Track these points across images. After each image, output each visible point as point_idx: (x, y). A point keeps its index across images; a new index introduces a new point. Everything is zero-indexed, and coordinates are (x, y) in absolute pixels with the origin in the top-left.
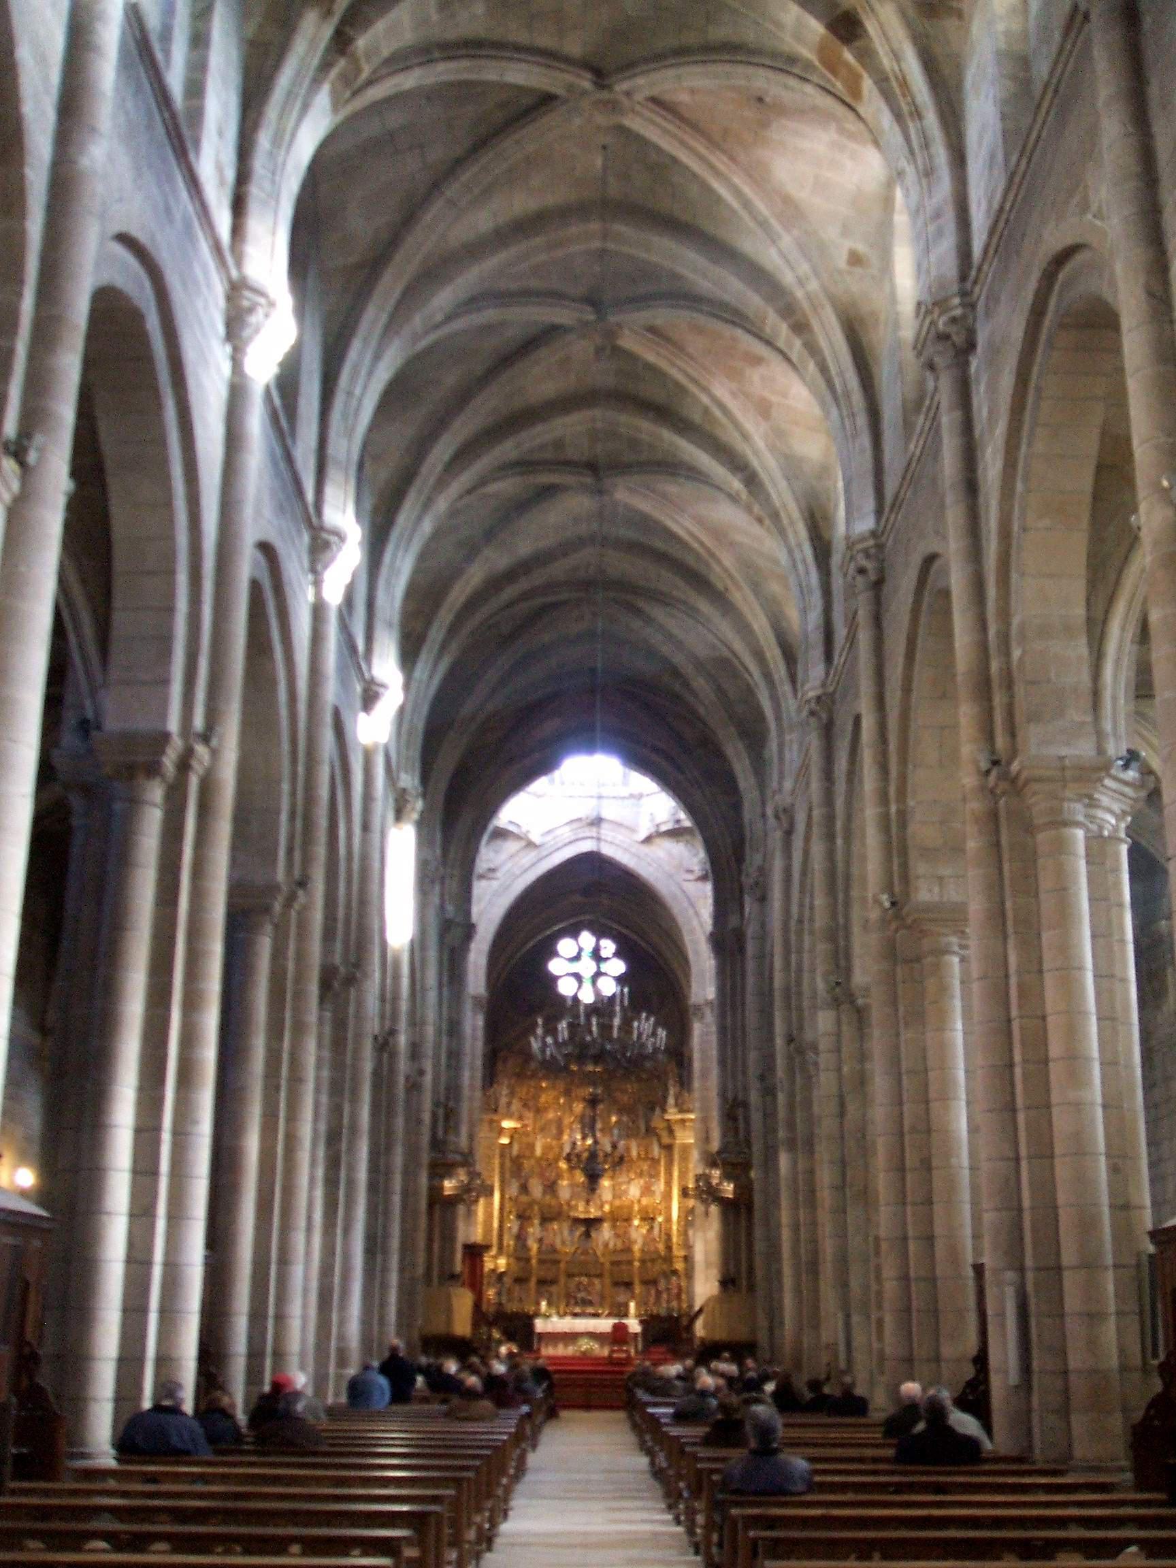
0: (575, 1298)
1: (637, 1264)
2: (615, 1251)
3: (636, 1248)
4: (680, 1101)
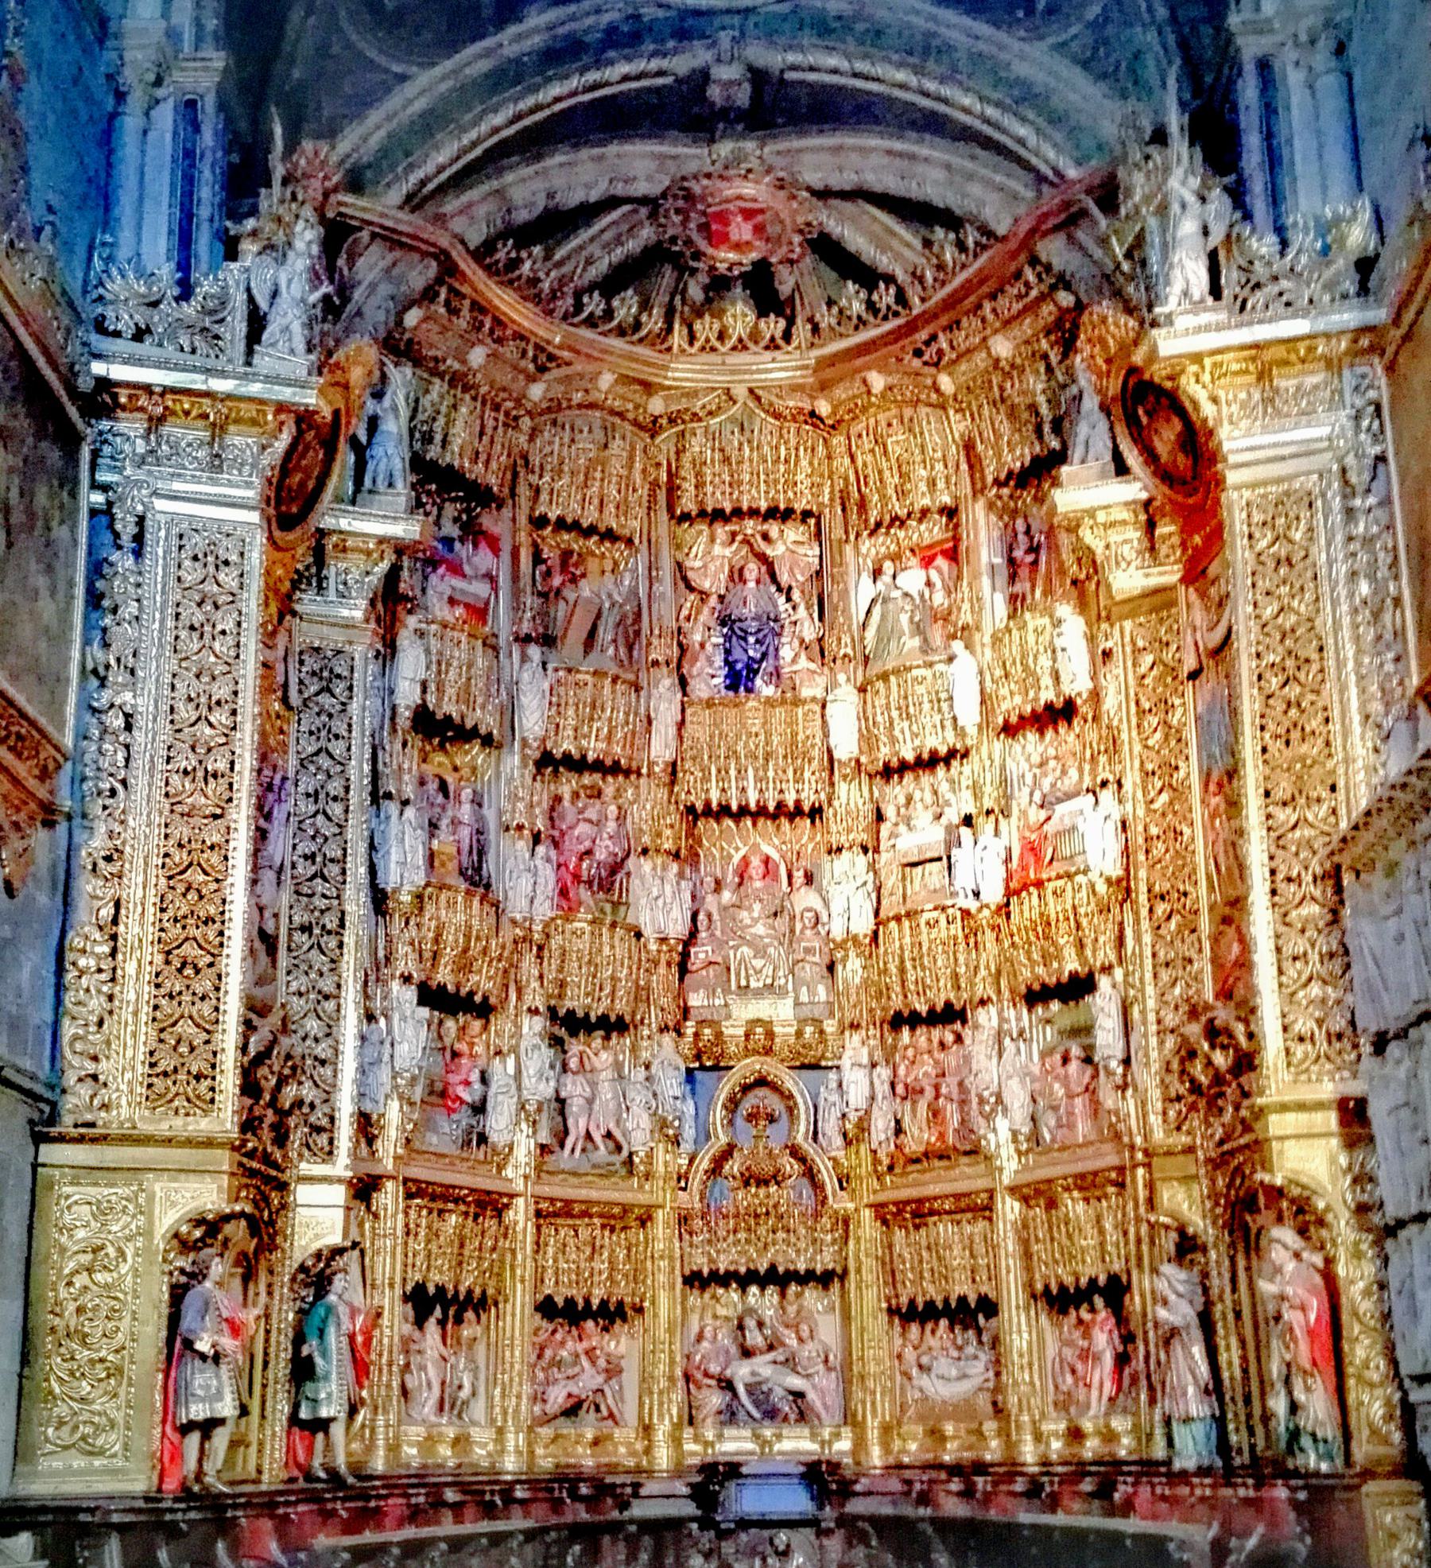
0: (727, 1385)
1: (1009, 1209)
2: (903, 1162)
4: (1230, 278)
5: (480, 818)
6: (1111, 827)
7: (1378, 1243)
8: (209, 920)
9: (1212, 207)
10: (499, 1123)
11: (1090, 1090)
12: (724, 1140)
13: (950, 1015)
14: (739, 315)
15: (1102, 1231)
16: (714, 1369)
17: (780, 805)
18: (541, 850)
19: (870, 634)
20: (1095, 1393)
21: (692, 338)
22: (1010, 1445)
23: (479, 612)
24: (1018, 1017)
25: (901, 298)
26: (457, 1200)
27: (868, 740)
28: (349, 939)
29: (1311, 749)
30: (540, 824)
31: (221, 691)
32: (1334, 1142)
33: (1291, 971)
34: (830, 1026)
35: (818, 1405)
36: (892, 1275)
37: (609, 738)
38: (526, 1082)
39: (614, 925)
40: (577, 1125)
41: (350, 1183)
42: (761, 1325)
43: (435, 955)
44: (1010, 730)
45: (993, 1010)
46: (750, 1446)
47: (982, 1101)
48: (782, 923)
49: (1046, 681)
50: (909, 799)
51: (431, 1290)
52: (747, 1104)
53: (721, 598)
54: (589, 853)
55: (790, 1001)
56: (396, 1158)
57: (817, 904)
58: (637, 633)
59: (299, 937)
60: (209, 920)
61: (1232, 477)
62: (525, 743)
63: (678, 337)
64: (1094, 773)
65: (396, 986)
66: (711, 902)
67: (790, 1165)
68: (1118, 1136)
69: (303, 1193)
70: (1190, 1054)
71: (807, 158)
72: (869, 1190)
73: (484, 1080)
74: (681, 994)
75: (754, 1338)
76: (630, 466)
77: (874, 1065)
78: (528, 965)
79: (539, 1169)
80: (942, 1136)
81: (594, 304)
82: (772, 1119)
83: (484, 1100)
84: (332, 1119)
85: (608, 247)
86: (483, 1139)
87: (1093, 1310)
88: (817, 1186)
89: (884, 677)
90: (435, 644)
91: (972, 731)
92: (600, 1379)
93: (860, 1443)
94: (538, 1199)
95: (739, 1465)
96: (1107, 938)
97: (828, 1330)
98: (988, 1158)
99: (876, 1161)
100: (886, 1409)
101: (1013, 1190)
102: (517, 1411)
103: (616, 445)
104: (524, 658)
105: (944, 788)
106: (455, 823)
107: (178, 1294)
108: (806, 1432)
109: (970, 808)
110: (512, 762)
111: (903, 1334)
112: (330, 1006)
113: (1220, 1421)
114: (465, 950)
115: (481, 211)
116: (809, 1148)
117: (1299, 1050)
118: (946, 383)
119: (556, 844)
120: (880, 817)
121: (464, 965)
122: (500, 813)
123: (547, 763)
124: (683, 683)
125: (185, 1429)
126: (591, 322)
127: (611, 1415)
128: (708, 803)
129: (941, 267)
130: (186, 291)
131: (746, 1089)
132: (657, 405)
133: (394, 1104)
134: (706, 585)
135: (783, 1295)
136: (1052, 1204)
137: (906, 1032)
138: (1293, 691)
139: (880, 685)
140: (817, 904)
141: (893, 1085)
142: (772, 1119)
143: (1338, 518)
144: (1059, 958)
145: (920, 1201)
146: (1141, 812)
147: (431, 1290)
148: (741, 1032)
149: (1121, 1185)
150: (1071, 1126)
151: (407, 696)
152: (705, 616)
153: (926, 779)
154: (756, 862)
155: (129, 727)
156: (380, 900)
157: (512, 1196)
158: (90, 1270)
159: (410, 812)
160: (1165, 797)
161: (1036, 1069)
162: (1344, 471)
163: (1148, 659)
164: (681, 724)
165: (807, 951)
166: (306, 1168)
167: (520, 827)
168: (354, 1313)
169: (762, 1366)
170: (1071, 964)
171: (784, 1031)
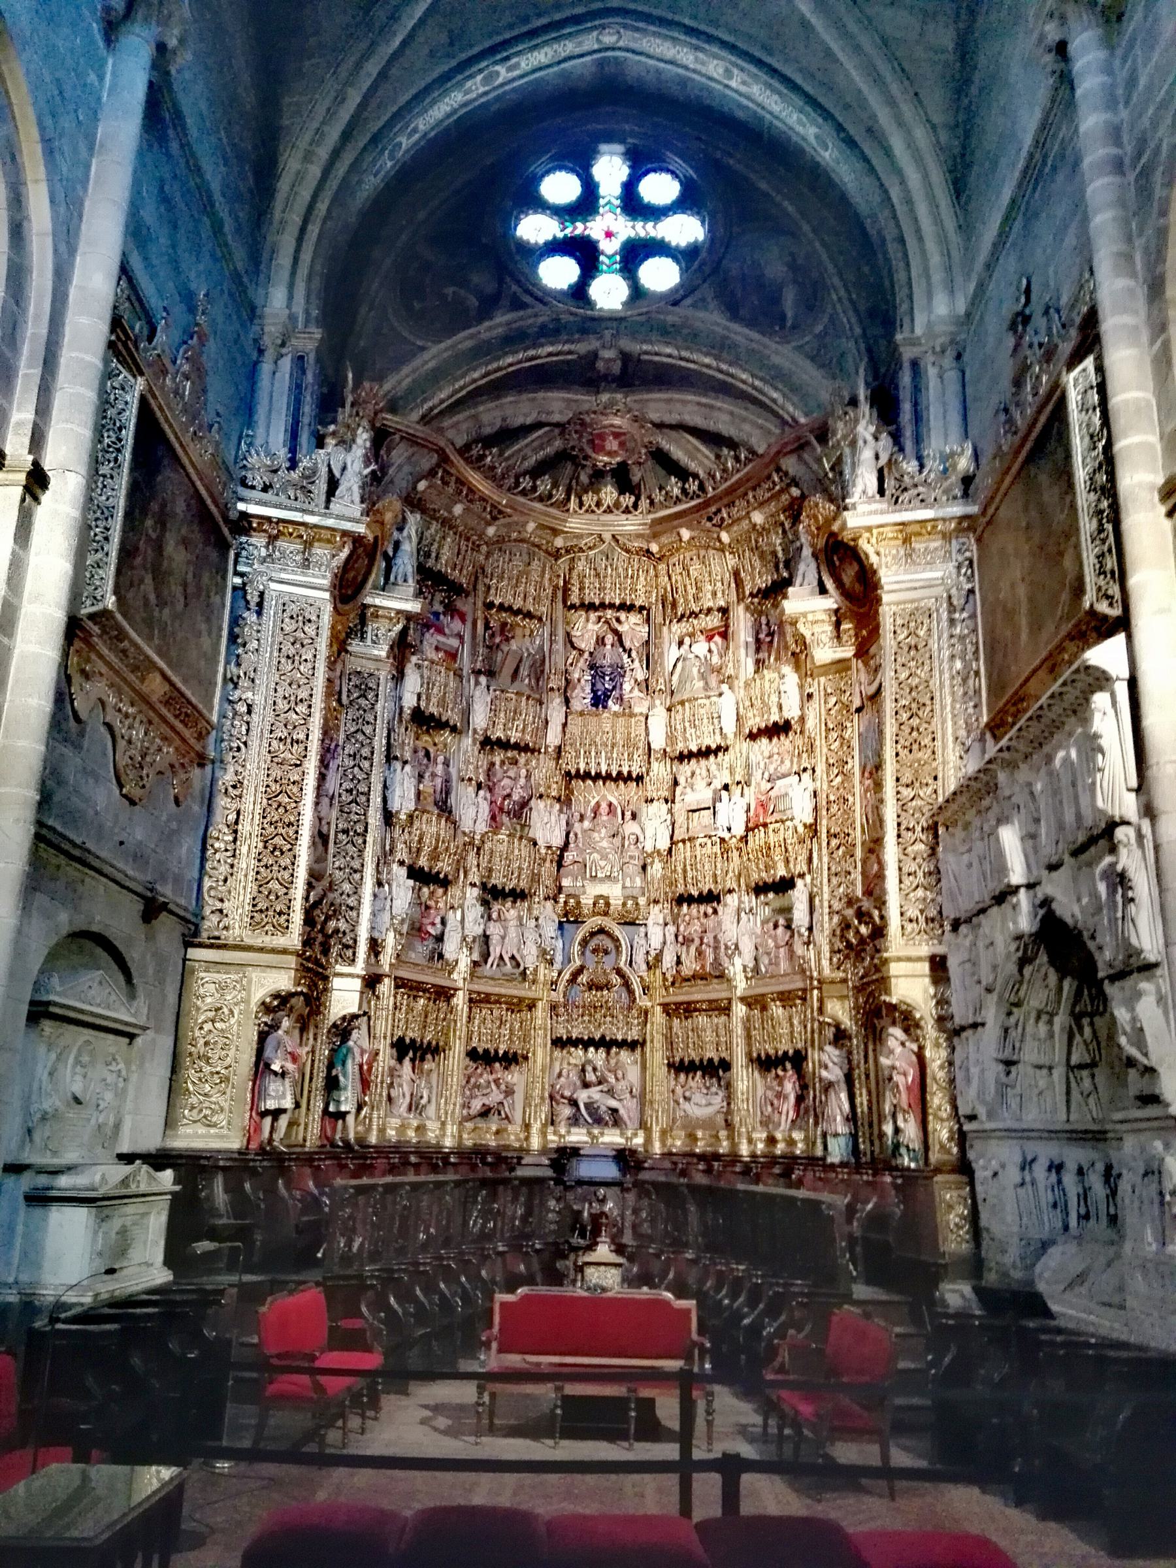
0: (574, 1103)
1: (739, 1010)
2: (680, 980)
3: (736, 968)
4: (890, 484)
5: (448, 773)
6: (808, 794)
7: (949, 1039)
8: (290, 824)
9: (881, 443)
10: (451, 948)
11: (789, 944)
12: (578, 963)
13: (711, 898)
14: (609, 493)
15: (792, 1025)
16: (567, 1093)
17: (620, 773)
18: (481, 793)
19: (675, 678)
20: (784, 1117)
21: (581, 505)
22: (734, 1145)
23: (452, 655)
24: (749, 901)
25: (702, 487)
26: (425, 991)
27: (671, 738)
28: (370, 839)
29: (924, 755)
30: (482, 778)
31: (302, 694)
32: (927, 980)
33: (907, 881)
34: (642, 901)
35: (625, 1117)
36: (670, 1043)
37: (523, 731)
38: (466, 925)
39: (521, 838)
40: (495, 951)
41: (363, 978)
42: (595, 1069)
43: (419, 850)
44: (752, 737)
45: (735, 895)
46: (586, 1139)
47: (727, 948)
48: (617, 841)
49: (775, 709)
50: (693, 774)
51: (408, 1041)
52: (592, 944)
53: (591, 654)
54: (509, 796)
55: (620, 885)
56: (391, 965)
57: (638, 832)
58: (542, 672)
59: (341, 836)
60: (290, 824)
61: (886, 598)
62: (475, 731)
63: (573, 504)
64: (799, 763)
65: (395, 866)
66: (577, 827)
67: (616, 979)
68: (803, 971)
69: (337, 983)
70: (846, 926)
71: (652, 405)
72: (660, 995)
73: (443, 922)
74: (558, 879)
75: (591, 1077)
76: (542, 576)
77: (666, 924)
78: (472, 859)
79: (472, 975)
80: (703, 967)
81: (526, 483)
82: (606, 952)
83: (443, 934)
84: (355, 941)
85: (536, 451)
86: (441, 956)
87: (785, 1070)
88: (631, 992)
89: (682, 703)
90: (426, 673)
91: (731, 736)
92: (502, 1096)
93: (648, 1140)
94: (471, 992)
95: (578, 1149)
96: (803, 858)
97: (633, 1074)
98: (729, 980)
99: (665, 979)
100: (664, 1121)
101: (743, 999)
102: (453, 1112)
103: (535, 564)
104: (477, 683)
105: (713, 768)
106: (433, 775)
107: (263, 1037)
108: (618, 1132)
109: (728, 780)
110: (467, 741)
111: (676, 1079)
112: (357, 876)
113: (854, 1136)
114: (436, 848)
115: (464, 426)
116: (626, 969)
117: (909, 927)
118: (725, 537)
119: (490, 790)
120: (676, 783)
121: (434, 856)
122: (459, 771)
123: (487, 744)
124: (567, 701)
125: (267, 1113)
126: (524, 493)
127: (507, 1117)
128: (578, 770)
129: (725, 470)
130: (293, 464)
131: (593, 934)
132: (559, 542)
133: (391, 935)
134: (583, 646)
135: (608, 1053)
136: (764, 1008)
137: (685, 906)
138: (915, 722)
139: (679, 707)
140: (638, 832)
141: (676, 936)
142: (606, 952)
143: (945, 624)
144: (774, 868)
145: (689, 1003)
146: (825, 787)
147: (408, 1041)
148: (591, 902)
149: (804, 999)
150: (777, 964)
151: (409, 701)
152: (581, 664)
153: (703, 762)
154: (604, 806)
155: (249, 712)
156: (388, 817)
157: (456, 990)
158: (213, 1021)
159: (408, 768)
160: (839, 779)
161: (759, 931)
162: (950, 597)
163: (833, 700)
164: (565, 725)
165: (631, 857)
166: (339, 968)
167: (470, 779)
168: (363, 1052)
169: (594, 1093)
170: (781, 872)
171: (616, 904)
